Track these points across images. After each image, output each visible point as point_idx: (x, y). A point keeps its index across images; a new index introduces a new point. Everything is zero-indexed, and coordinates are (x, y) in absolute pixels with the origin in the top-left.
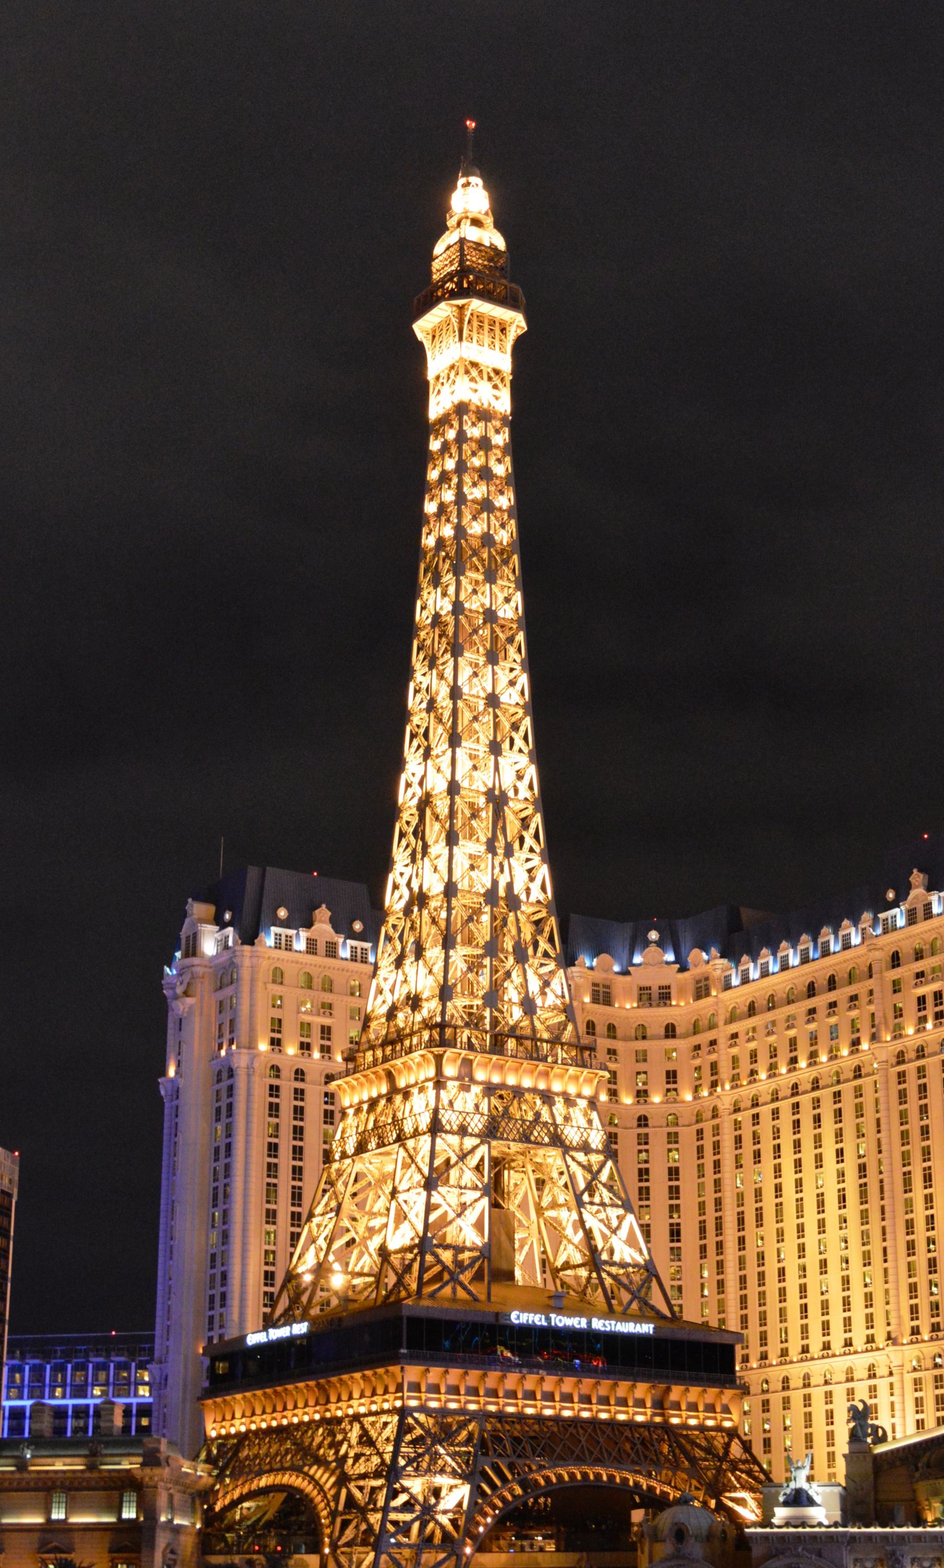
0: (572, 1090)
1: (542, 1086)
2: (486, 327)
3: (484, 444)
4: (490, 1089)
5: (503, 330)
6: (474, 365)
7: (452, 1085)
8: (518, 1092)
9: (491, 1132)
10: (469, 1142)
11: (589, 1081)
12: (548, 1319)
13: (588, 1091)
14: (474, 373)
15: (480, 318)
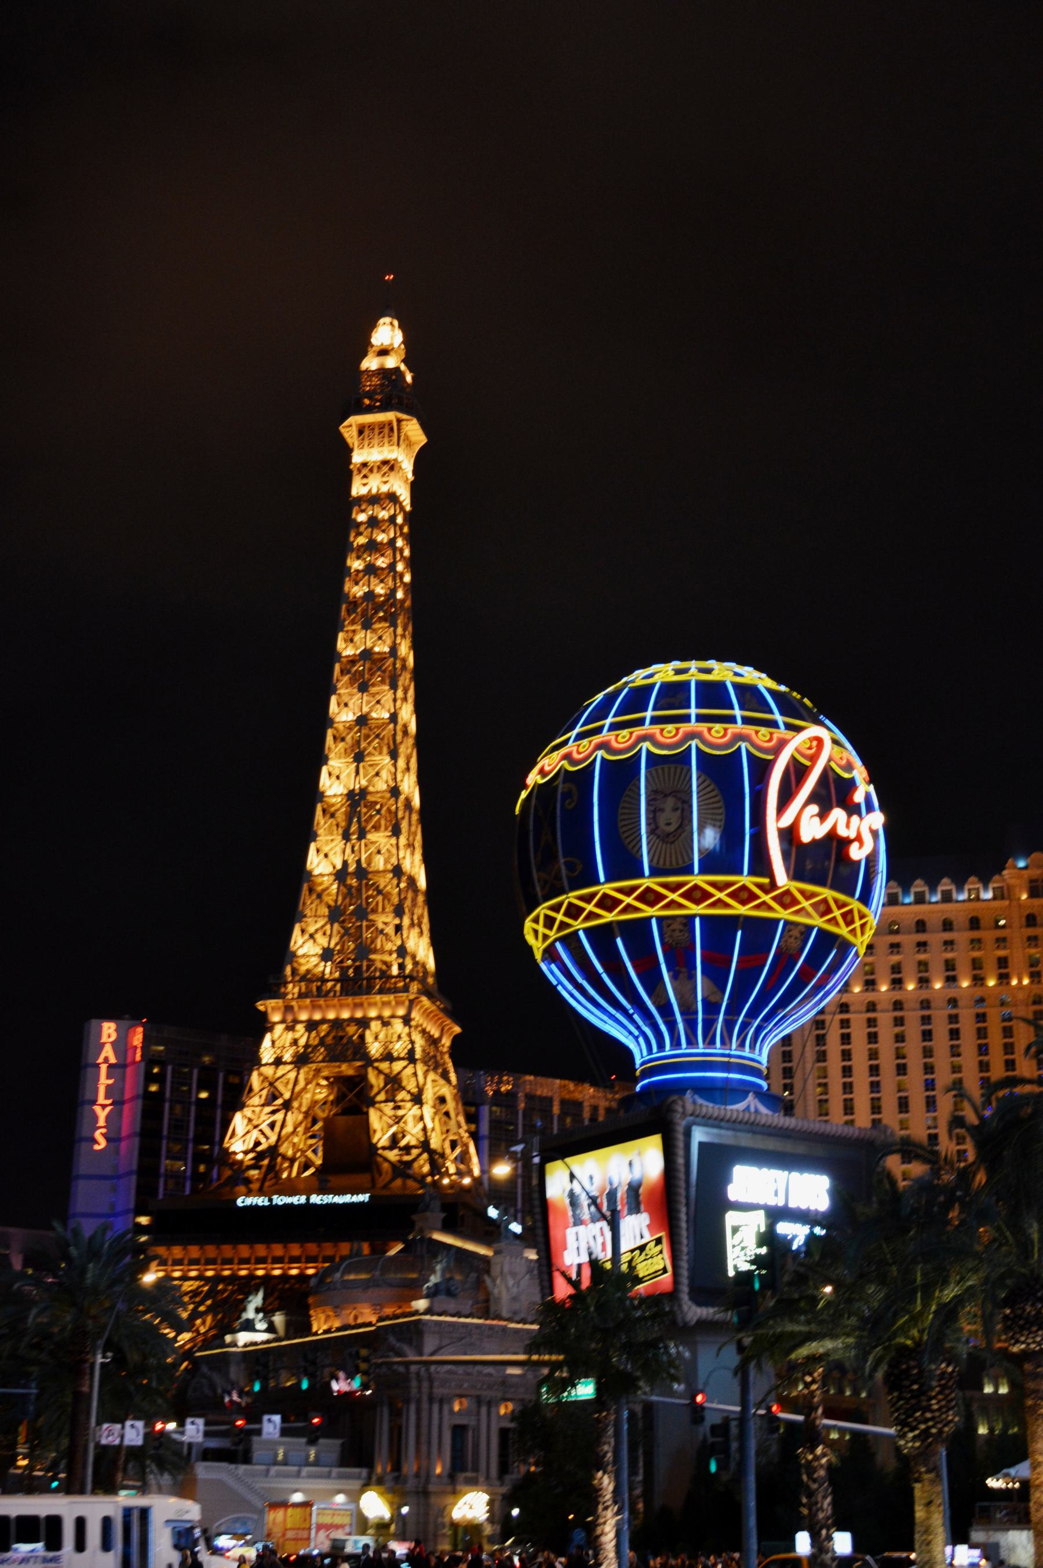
0: (387, 1013)
1: (359, 1014)
2: (377, 431)
3: (373, 522)
4: (311, 1026)
5: (392, 430)
6: (365, 465)
7: (279, 1029)
8: (337, 1024)
9: (301, 1060)
10: (282, 1070)
11: (399, 1003)
12: (271, 1200)
13: (401, 1012)
14: (365, 471)
15: (371, 427)
